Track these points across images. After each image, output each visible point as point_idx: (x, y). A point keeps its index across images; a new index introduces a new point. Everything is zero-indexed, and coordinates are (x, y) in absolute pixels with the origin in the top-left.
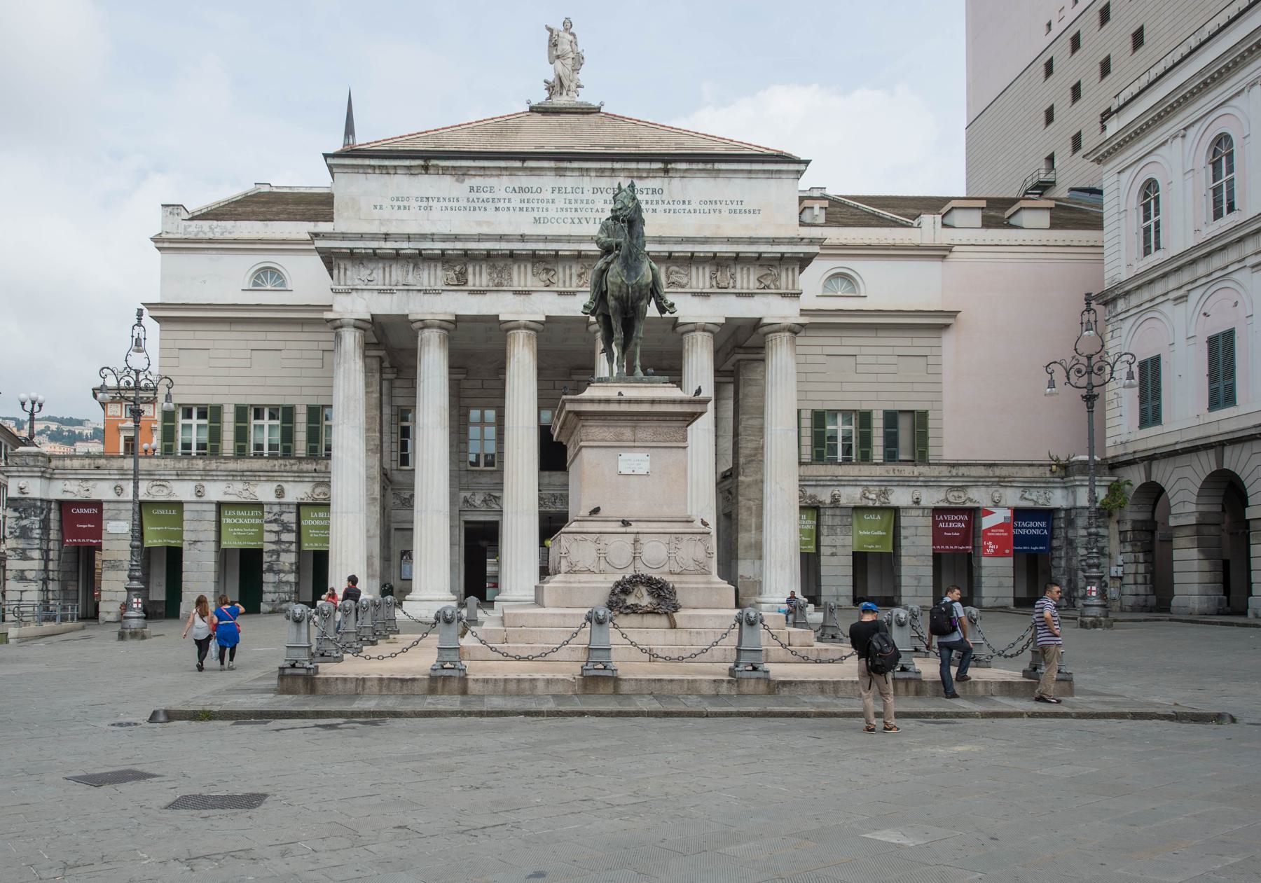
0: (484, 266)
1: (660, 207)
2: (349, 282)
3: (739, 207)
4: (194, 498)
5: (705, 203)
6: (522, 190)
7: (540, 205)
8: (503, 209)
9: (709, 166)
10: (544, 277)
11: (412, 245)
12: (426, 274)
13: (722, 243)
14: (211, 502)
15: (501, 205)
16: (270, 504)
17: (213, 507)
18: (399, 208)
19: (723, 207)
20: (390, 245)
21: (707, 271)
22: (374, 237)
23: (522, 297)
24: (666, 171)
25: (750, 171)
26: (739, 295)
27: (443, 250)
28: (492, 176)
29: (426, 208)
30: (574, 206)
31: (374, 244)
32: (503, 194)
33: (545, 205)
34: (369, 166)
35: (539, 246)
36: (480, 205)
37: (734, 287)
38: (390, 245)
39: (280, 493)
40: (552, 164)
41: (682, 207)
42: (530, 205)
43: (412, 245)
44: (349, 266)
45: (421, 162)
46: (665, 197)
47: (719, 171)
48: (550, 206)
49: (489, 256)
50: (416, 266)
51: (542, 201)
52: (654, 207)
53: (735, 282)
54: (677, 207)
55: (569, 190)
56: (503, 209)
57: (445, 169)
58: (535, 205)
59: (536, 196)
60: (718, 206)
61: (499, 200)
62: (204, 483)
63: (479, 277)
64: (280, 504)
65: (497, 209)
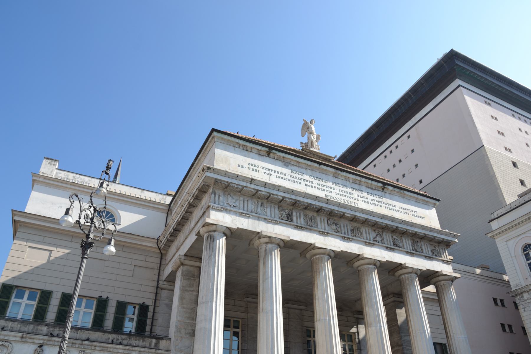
0: (302, 213)
1: (382, 205)
2: (221, 203)
3: (415, 214)
5: (402, 208)
7: (327, 189)
8: (309, 186)
9: (402, 191)
10: (334, 227)
11: (266, 190)
12: (269, 210)
13: (419, 228)
15: (308, 183)
18: (253, 170)
20: (252, 186)
21: (410, 241)
22: (245, 179)
24: (383, 189)
25: (417, 199)
27: (284, 198)
28: (302, 168)
29: (268, 174)
31: (244, 184)
33: (330, 190)
34: (238, 143)
35: (336, 208)
36: (298, 180)
38: (252, 186)
42: (323, 188)
43: (266, 190)
44: (221, 194)
45: (267, 149)
47: (405, 194)
48: (332, 190)
49: (307, 207)
50: (262, 204)
51: (329, 187)
52: (381, 204)
53: (422, 250)
57: (281, 156)
58: (325, 188)
60: (407, 211)
63: (298, 219)
65: (306, 185)
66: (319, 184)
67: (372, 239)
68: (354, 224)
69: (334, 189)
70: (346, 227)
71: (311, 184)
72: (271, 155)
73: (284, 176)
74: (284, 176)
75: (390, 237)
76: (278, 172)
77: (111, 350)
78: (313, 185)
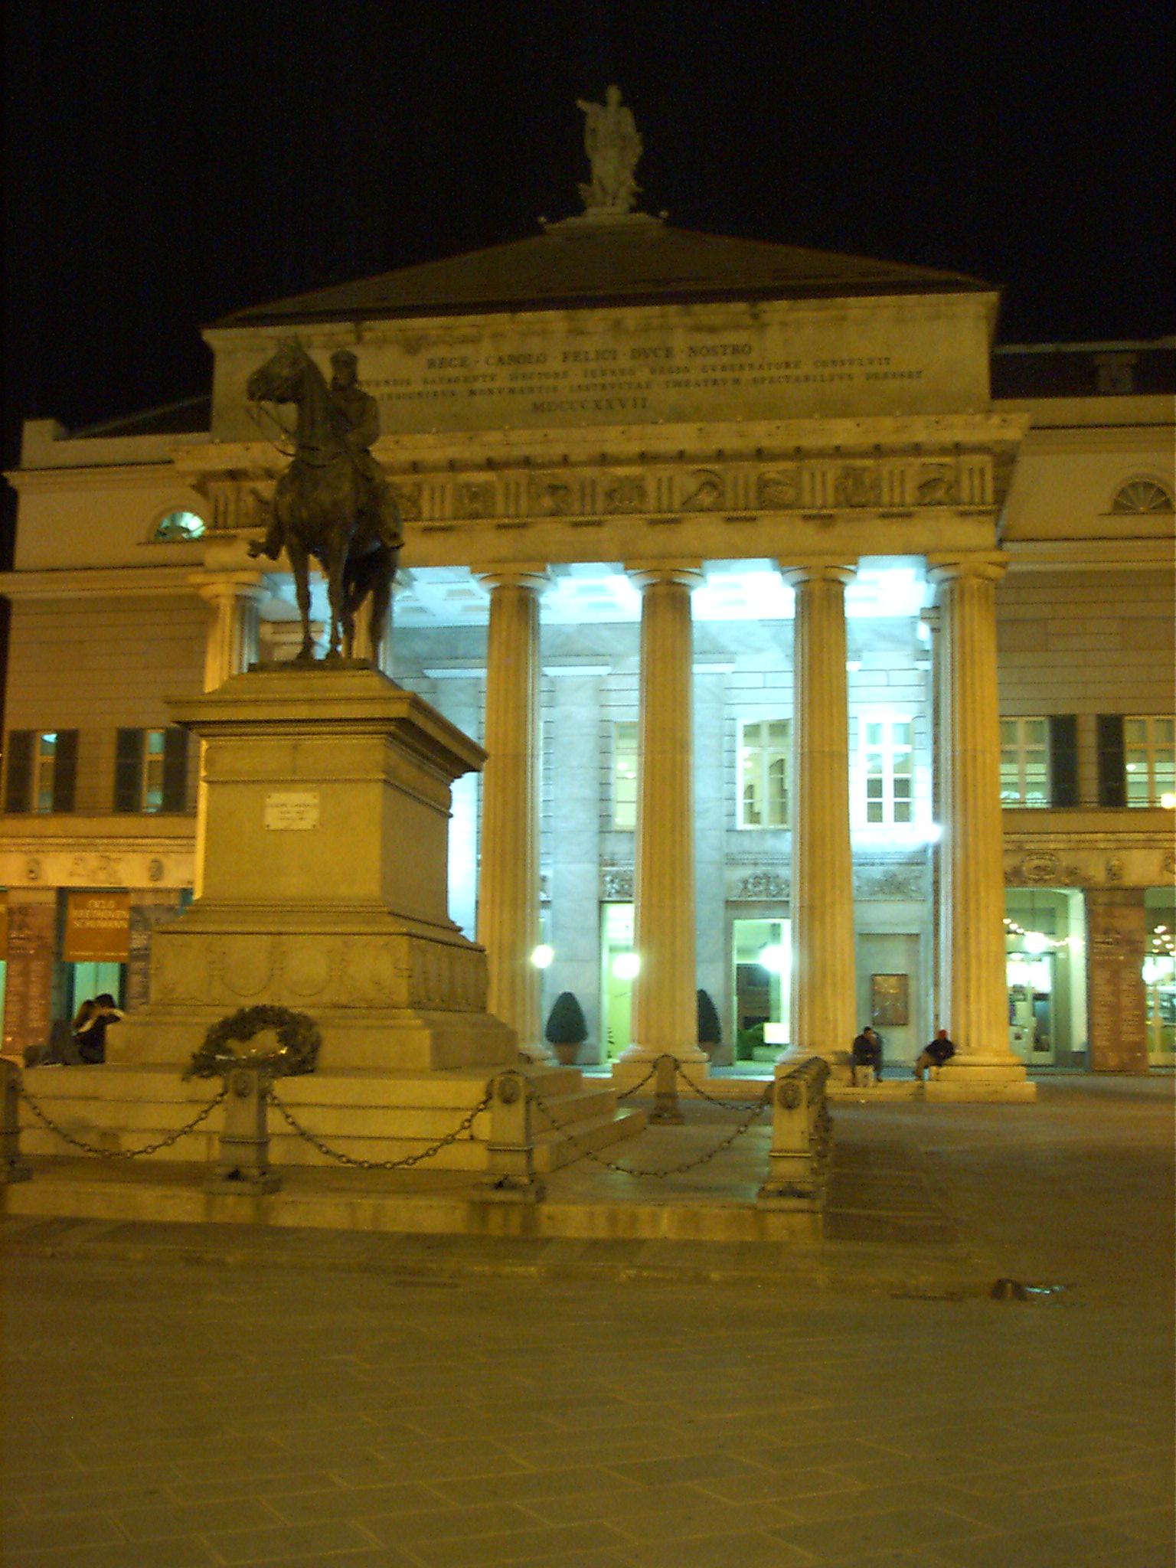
1: (747, 375)
3: (885, 368)
4: (26, 883)
5: (825, 364)
6: (515, 359)
10: (547, 502)
14: (49, 889)
15: (478, 386)
16: (140, 891)
17: (51, 897)
19: (855, 370)
23: (513, 532)
24: (755, 316)
26: (884, 516)
28: (464, 340)
30: (600, 380)
32: (481, 369)
33: (551, 382)
37: (878, 504)
39: (157, 871)
40: (561, 313)
41: (783, 372)
46: (754, 357)
51: (547, 376)
52: (737, 375)
54: (774, 372)
55: (592, 355)
56: (482, 392)
59: (541, 368)
60: (846, 370)
61: (476, 378)
62: (40, 857)
64: (156, 891)
65: (472, 393)
66: (513, 377)
67: (677, 505)
68: (621, 471)
69: (565, 375)
70: (588, 490)
71: (489, 385)
72: (368, 336)
73: (402, 389)
74: (402, 389)
75: (753, 478)
76: (387, 382)
77: (156, 849)
78: (495, 385)
